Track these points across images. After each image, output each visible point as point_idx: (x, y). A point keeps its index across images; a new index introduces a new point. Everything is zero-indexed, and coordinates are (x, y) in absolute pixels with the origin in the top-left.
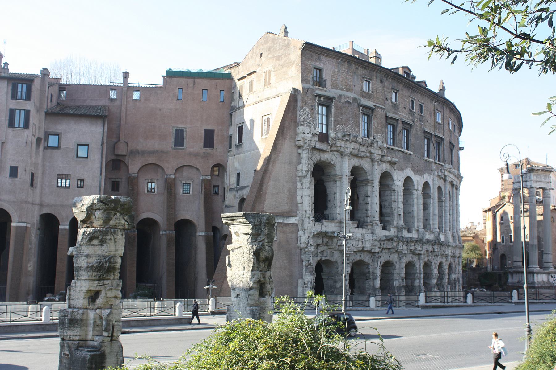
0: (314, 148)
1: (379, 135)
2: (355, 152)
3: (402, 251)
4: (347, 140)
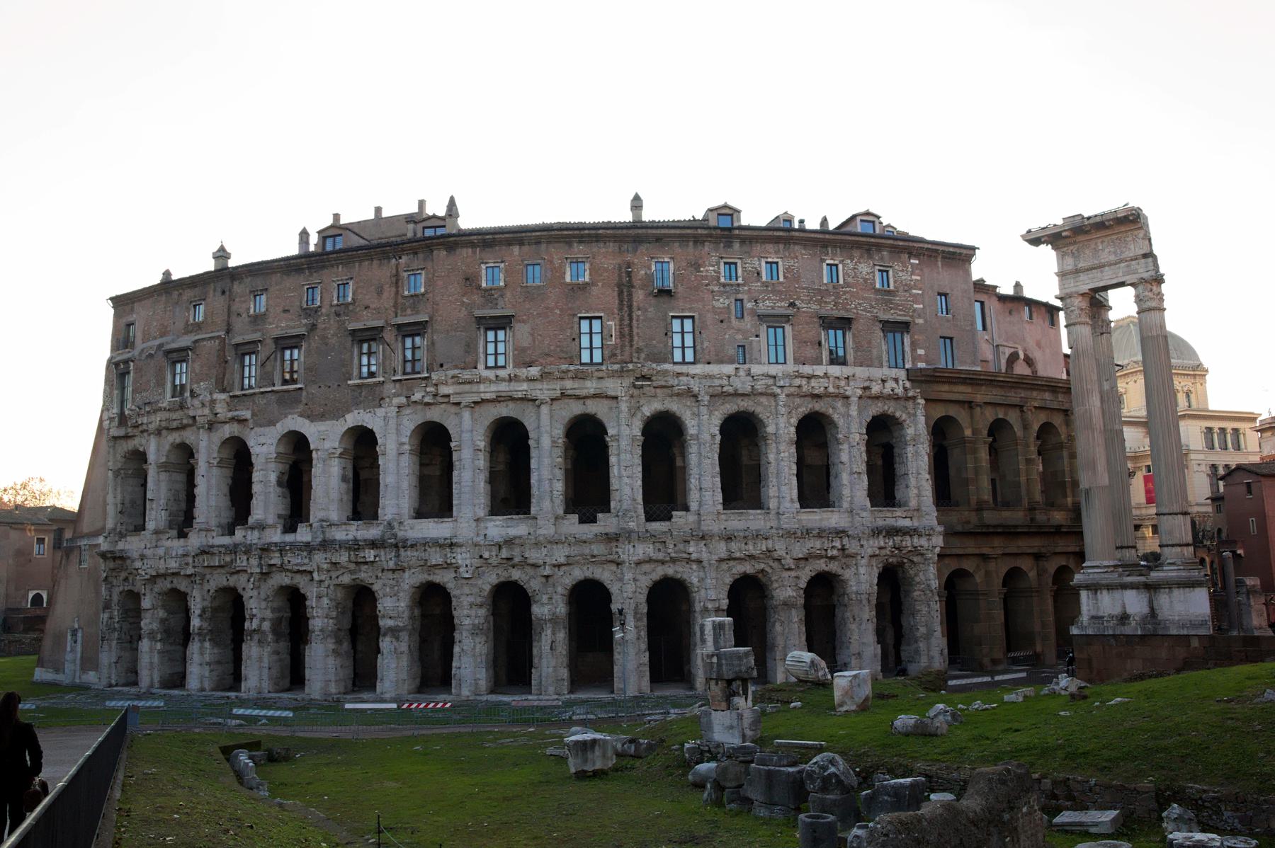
0: (115, 438)
1: (202, 383)
2: (164, 424)
3: (245, 568)
4: (148, 412)
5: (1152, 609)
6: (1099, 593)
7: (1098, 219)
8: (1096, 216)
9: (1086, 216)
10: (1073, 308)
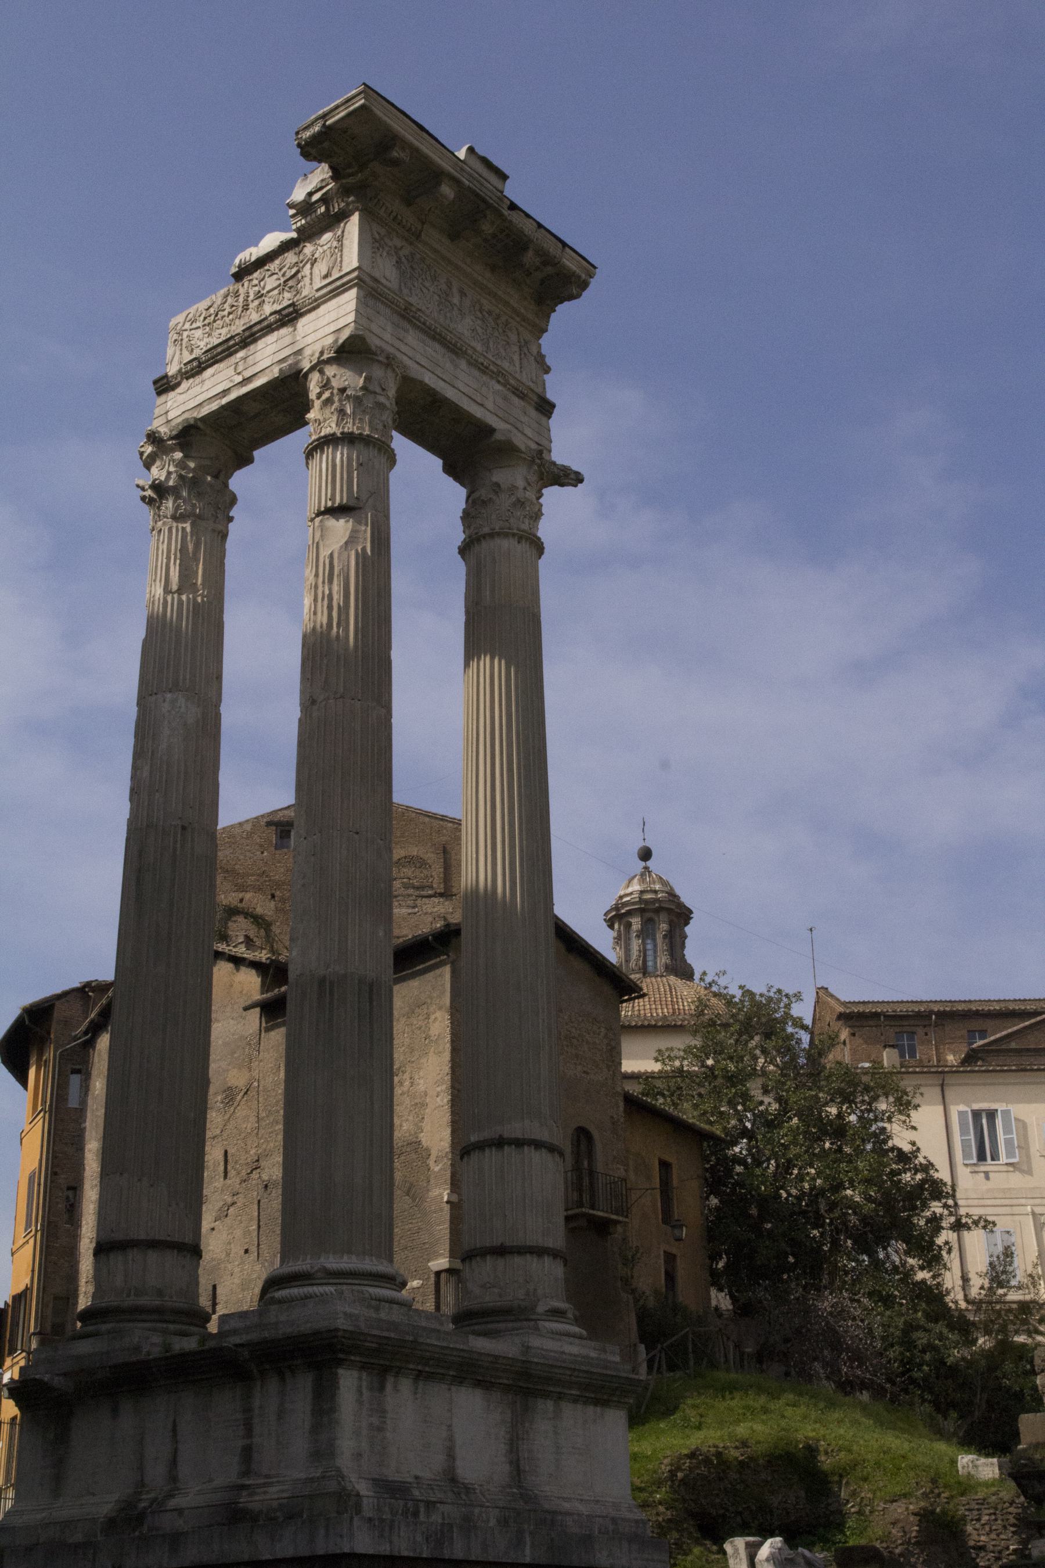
5: (517, 1470)
6: (390, 1381)
7: (528, 227)
8: (528, 216)
9: (512, 191)
10: (382, 399)
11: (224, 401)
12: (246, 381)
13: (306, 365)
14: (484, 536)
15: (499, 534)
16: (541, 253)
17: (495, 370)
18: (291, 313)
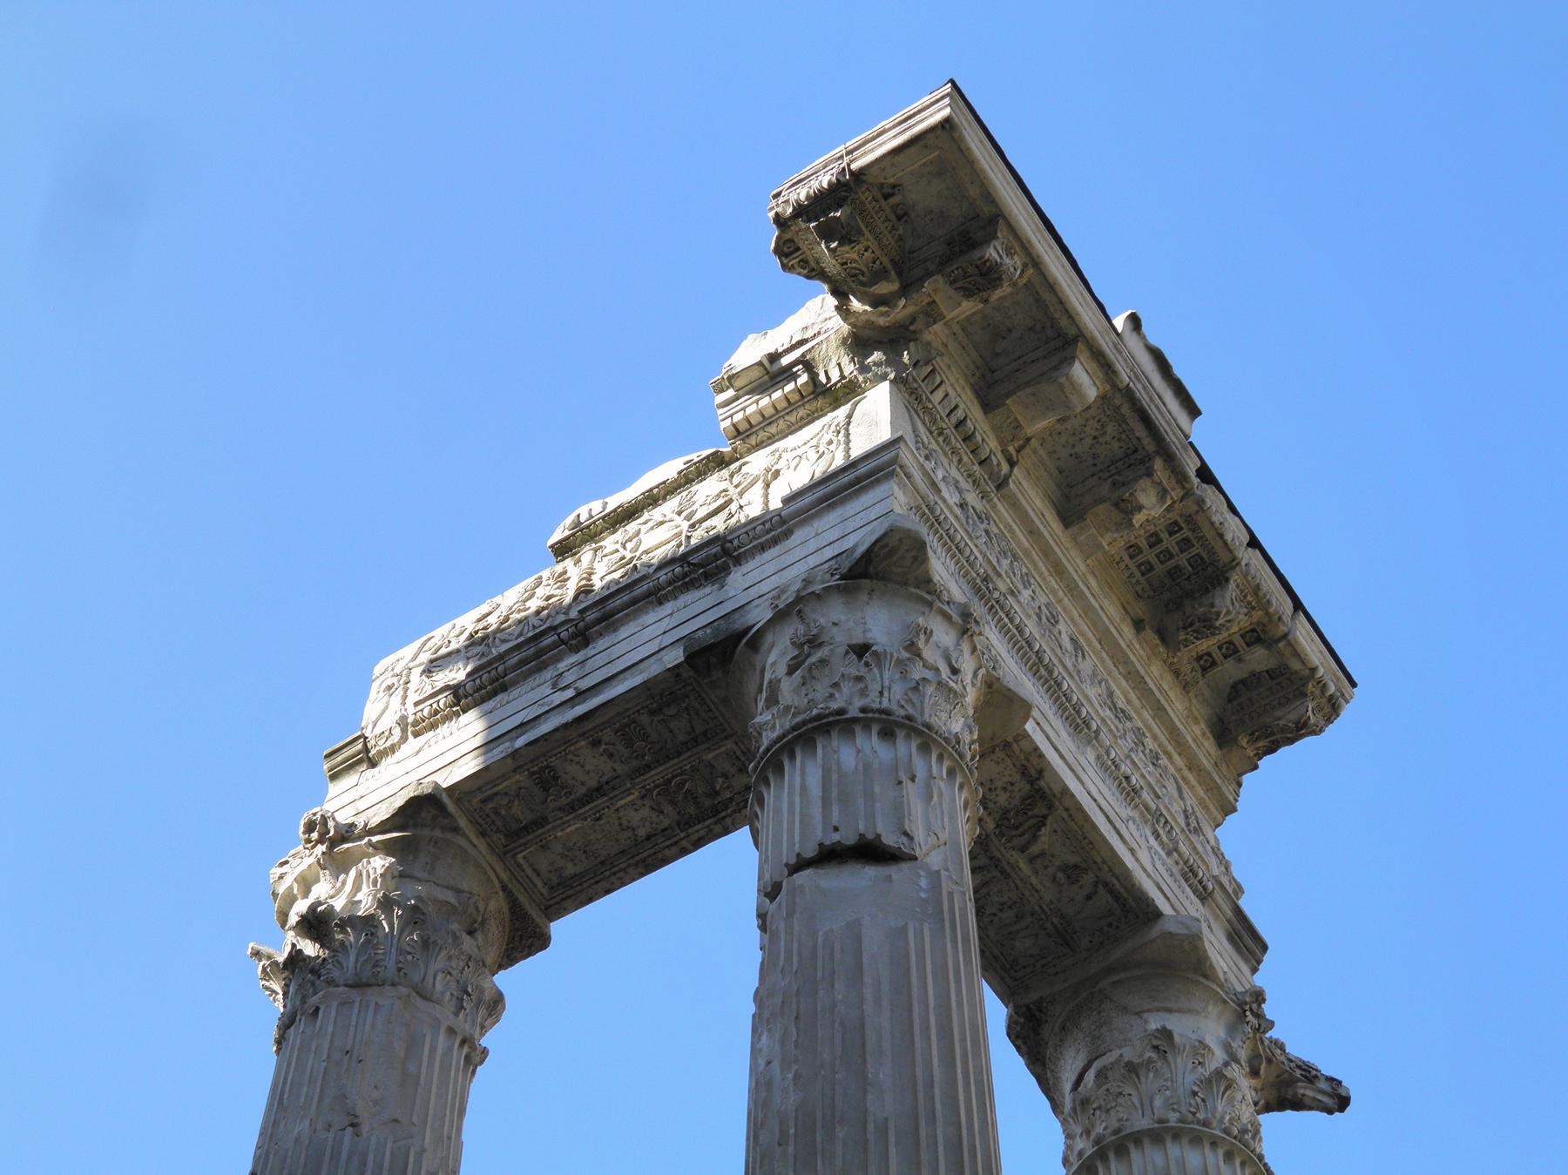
7: (1234, 532)
11: (520, 742)
12: (581, 695)
13: (760, 615)
14: (1137, 1138)
15: (1176, 1135)
16: (1255, 597)
17: (1154, 807)
18: (716, 557)
